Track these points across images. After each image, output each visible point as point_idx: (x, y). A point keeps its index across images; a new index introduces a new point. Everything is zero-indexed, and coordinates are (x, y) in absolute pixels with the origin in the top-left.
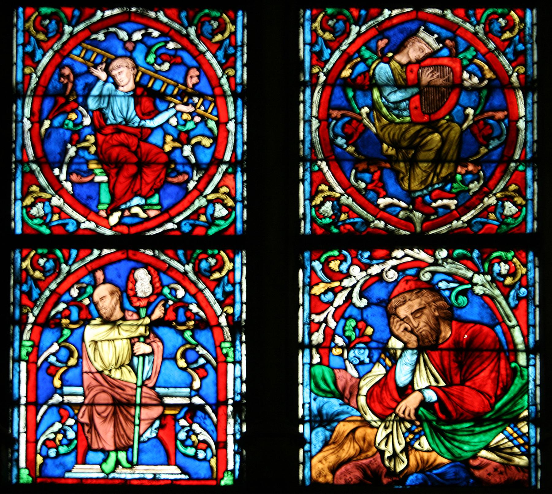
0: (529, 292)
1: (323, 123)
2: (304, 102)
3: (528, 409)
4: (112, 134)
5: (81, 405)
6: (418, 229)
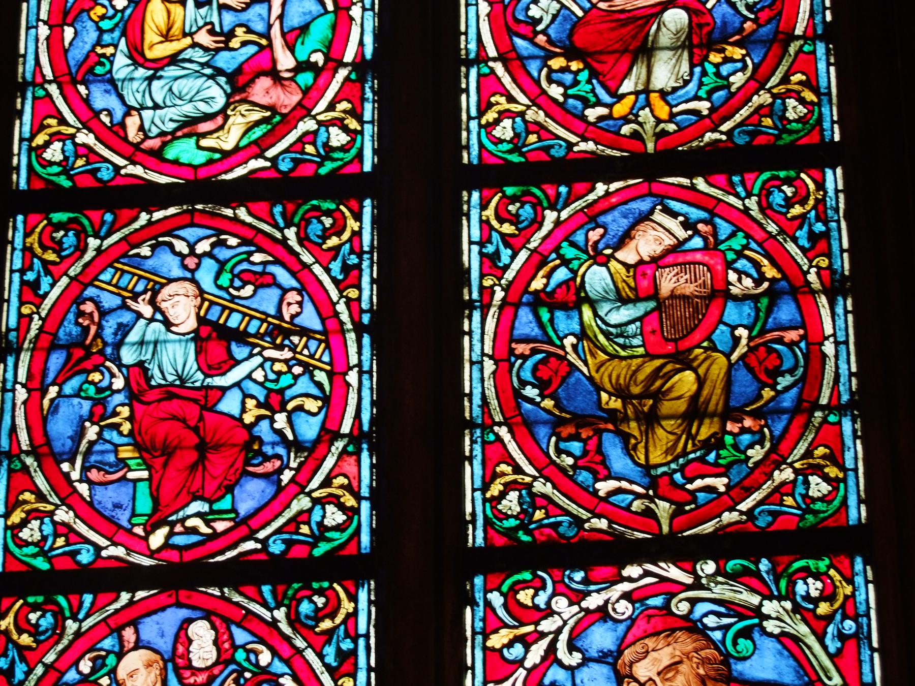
0: (859, 626)
1: (500, 364)
2: (470, 333)
4: (159, 401)
6: (665, 529)
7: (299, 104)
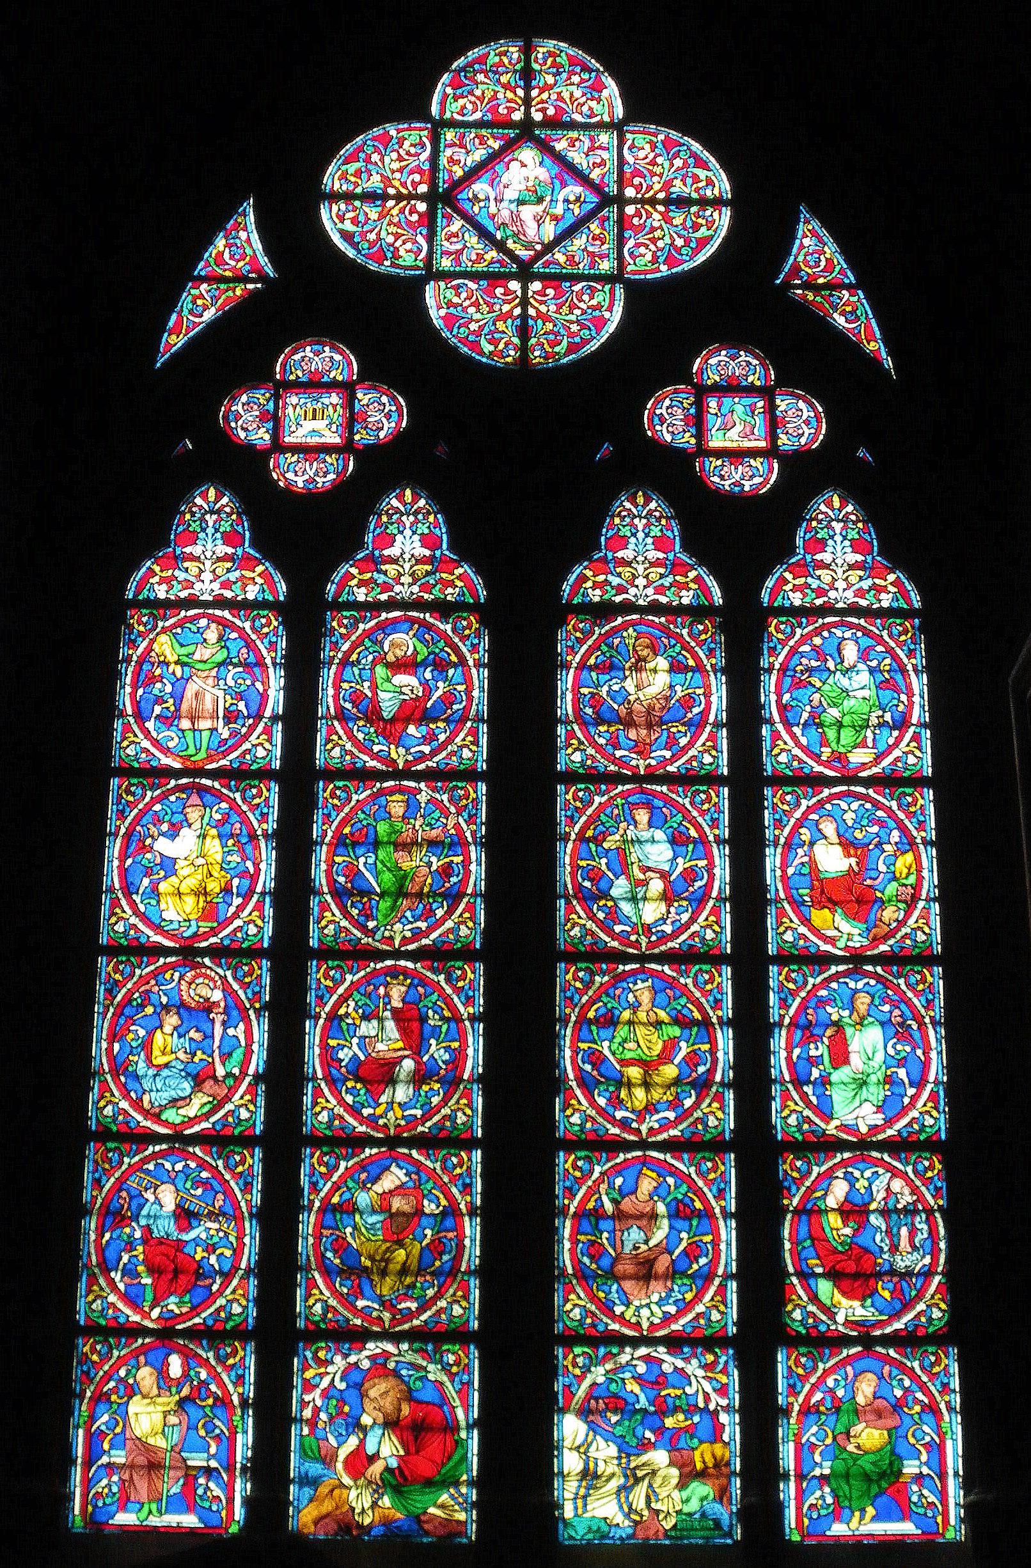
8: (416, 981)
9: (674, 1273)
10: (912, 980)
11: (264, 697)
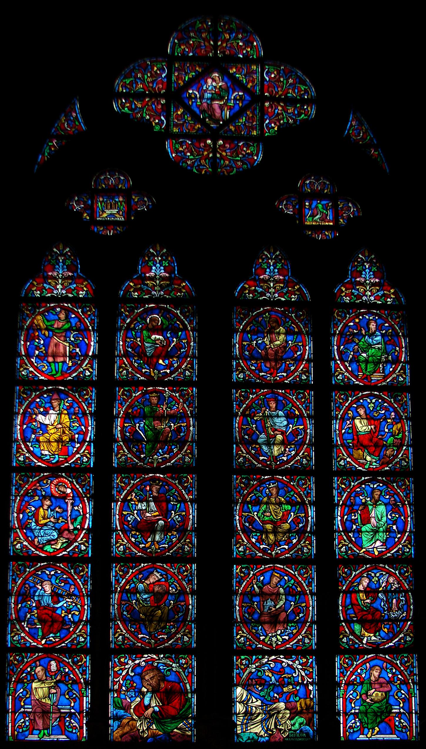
2: (112, 598)
3: (192, 714)
5: (31, 712)
7: (74, 538)
8: (164, 483)
9: (287, 621)
10: (400, 484)
11: (88, 346)
